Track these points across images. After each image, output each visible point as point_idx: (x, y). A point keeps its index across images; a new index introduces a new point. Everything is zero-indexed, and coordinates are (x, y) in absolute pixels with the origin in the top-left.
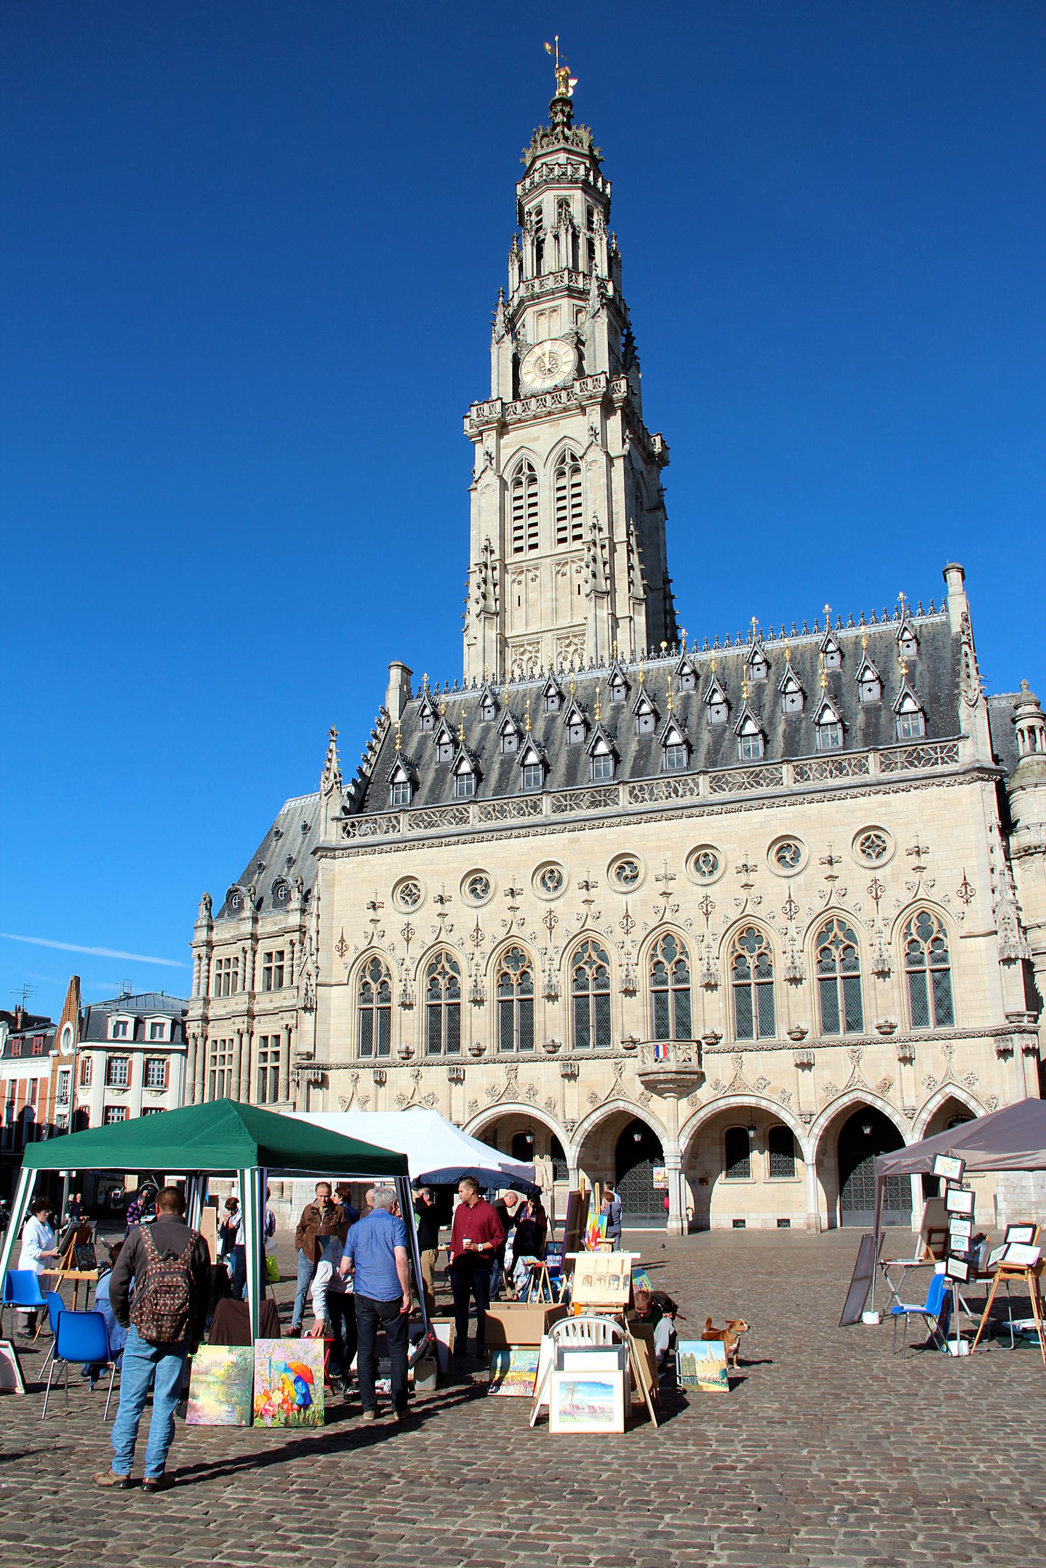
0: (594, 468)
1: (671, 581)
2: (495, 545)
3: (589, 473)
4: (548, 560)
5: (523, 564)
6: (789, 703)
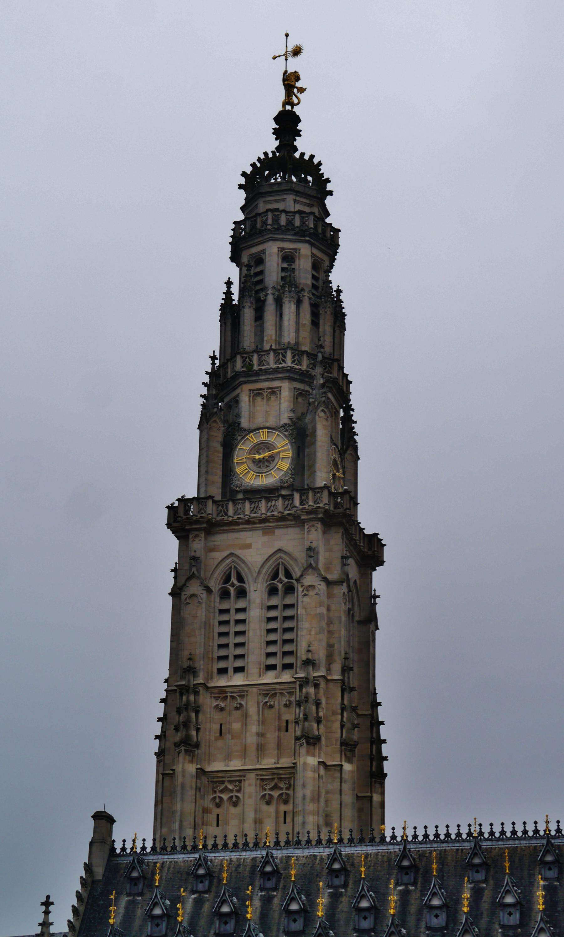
0: (311, 593)
1: (379, 704)
2: (200, 664)
3: (306, 599)
4: (255, 690)
5: (228, 690)
6: (506, 916)
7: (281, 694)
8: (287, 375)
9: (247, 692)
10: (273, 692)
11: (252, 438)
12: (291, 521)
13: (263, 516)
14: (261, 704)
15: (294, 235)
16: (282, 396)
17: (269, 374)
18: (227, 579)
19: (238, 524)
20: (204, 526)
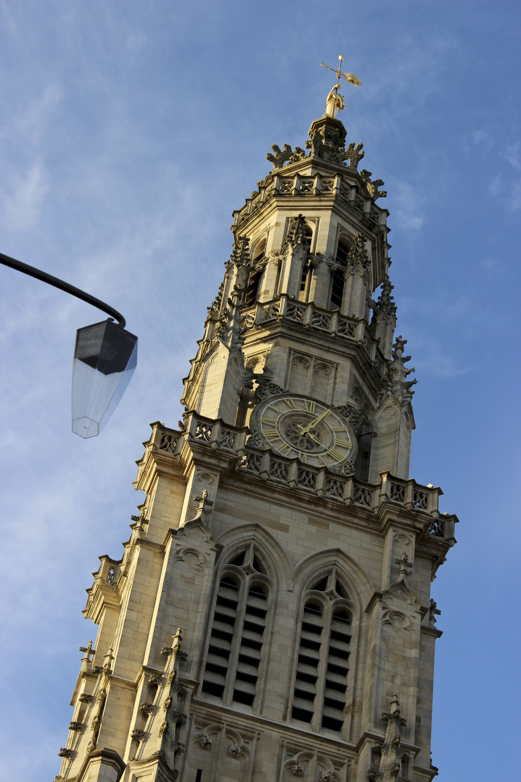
4: (276, 734)
5: (226, 717)
7: (320, 759)
8: (353, 353)
9: (259, 734)
10: (306, 751)
11: (291, 404)
12: (361, 519)
13: (320, 493)
14: (283, 763)
15: (360, 222)
16: (338, 375)
17: (326, 341)
18: (239, 560)
19: (273, 491)
20: (225, 465)
